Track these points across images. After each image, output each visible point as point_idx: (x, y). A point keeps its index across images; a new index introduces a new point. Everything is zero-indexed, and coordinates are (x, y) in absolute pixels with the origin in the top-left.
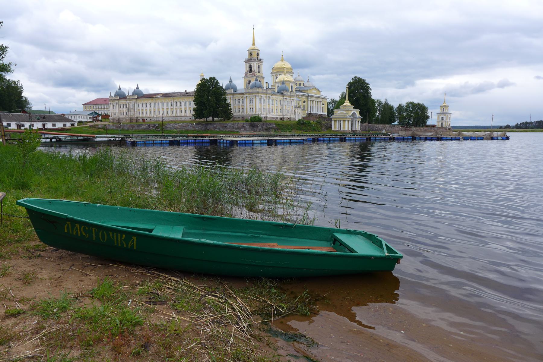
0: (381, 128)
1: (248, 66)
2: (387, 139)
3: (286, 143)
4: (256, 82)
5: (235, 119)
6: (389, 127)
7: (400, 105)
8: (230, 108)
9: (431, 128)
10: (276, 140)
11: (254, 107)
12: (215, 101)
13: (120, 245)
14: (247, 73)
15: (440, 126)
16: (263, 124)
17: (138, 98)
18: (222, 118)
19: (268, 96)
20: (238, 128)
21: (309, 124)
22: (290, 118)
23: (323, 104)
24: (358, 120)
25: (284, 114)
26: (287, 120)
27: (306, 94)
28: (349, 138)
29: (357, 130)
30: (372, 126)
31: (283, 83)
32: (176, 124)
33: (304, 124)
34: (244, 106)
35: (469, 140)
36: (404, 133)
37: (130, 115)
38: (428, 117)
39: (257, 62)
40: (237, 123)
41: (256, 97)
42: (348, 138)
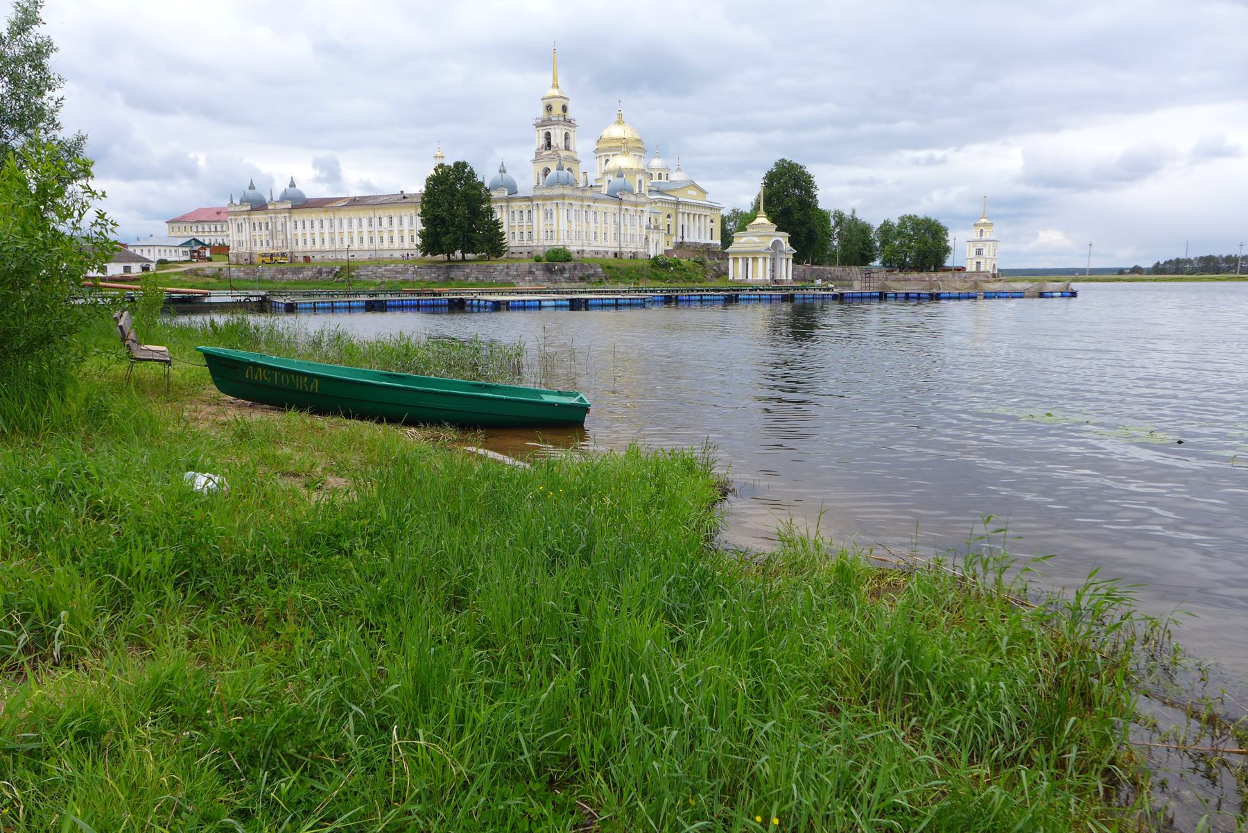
0: (839, 274)
1: (542, 134)
3: (609, 305)
4: (560, 172)
5: (513, 256)
8: (500, 230)
9: (953, 274)
10: (587, 300)
11: (555, 228)
15: (974, 269)
16: (575, 267)
17: (294, 207)
18: (484, 254)
19: (586, 203)
20: (518, 275)
21: (678, 266)
23: (712, 221)
25: (622, 243)
27: (674, 199)
28: (745, 297)
29: (785, 278)
31: (620, 173)
32: (380, 268)
33: (666, 266)
35: (994, 297)
36: (863, 285)
38: (947, 250)
39: (563, 127)
40: (516, 264)
41: (560, 206)
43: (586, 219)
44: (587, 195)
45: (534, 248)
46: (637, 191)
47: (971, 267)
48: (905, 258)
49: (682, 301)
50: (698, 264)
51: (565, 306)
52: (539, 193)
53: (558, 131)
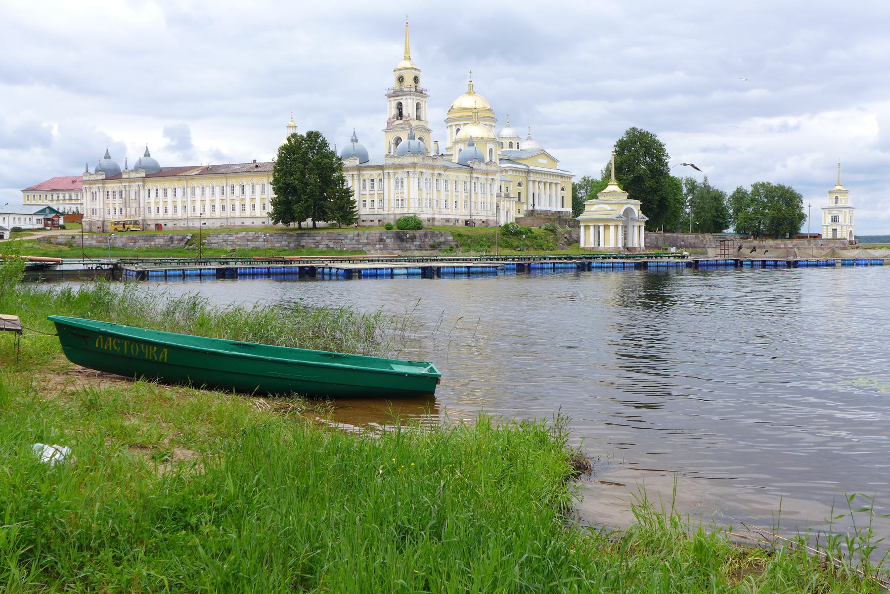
0: (693, 241)
1: (394, 104)
2: (682, 266)
3: (461, 273)
4: (411, 141)
5: (364, 224)
6: (712, 239)
7: (738, 189)
8: (351, 199)
10: (439, 268)
11: (405, 196)
13: (151, 358)
14: (392, 120)
15: (830, 236)
16: (426, 235)
17: (147, 176)
19: (436, 172)
20: (369, 243)
22: (487, 220)
23: (563, 189)
25: (473, 211)
26: (481, 224)
27: (525, 167)
28: (598, 264)
29: (637, 245)
30: (673, 237)
31: (471, 142)
32: (231, 235)
33: (517, 234)
34: (383, 194)
35: (853, 265)
36: (718, 252)
37: (128, 214)
38: (802, 217)
39: (414, 97)
40: (367, 232)
41: (411, 175)
42: (595, 264)
45: (385, 216)
46: (487, 159)
47: (827, 234)
48: (759, 225)
49: (535, 269)
50: (549, 232)
51: (418, 274)
52: (390, 161)
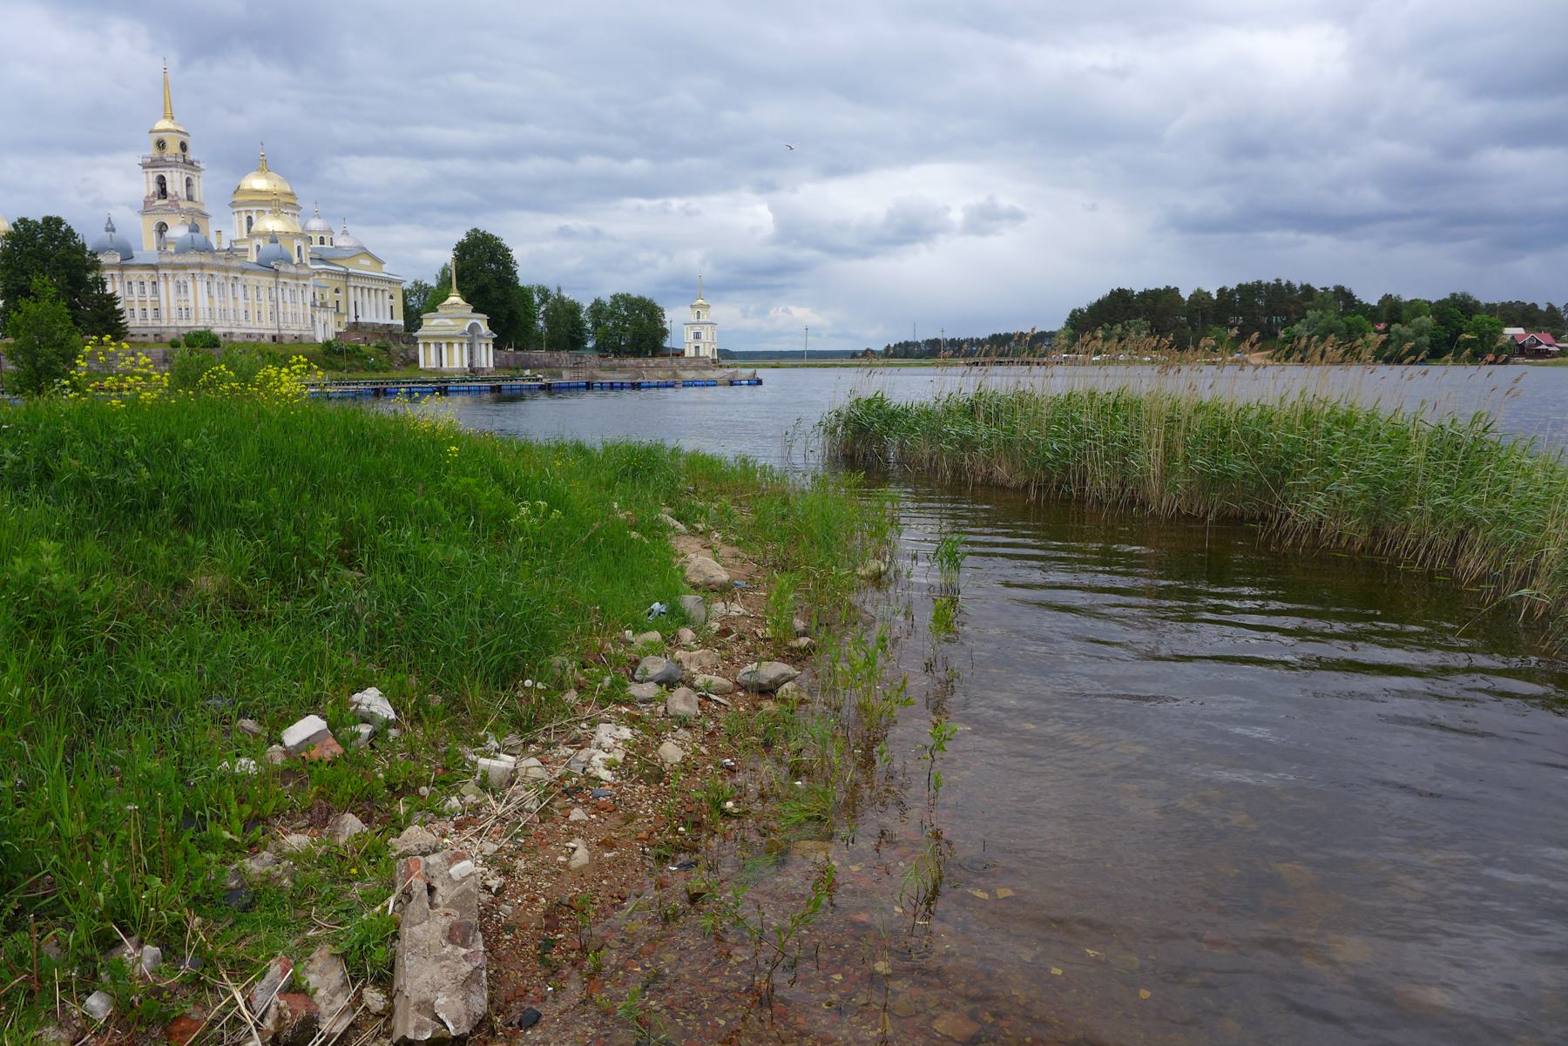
1: (152, 176)
4: (195, 235)
5: (133, 339)
8: (118, 307)
11: (191, 304)
12: (70, 288)
15: (693, 355)
19: (231, 275)
21: (357, 353)
23: (391, 297)
24: (484, 341)
27: (342, 269)
31: (274, 238)
38: (664, 333)
39: (182, 170)
43: (233, 294)
44: (226, 263)
45: (163, 330)
46: (296, 260)
52: (166, 260)
53: (176, 175)
